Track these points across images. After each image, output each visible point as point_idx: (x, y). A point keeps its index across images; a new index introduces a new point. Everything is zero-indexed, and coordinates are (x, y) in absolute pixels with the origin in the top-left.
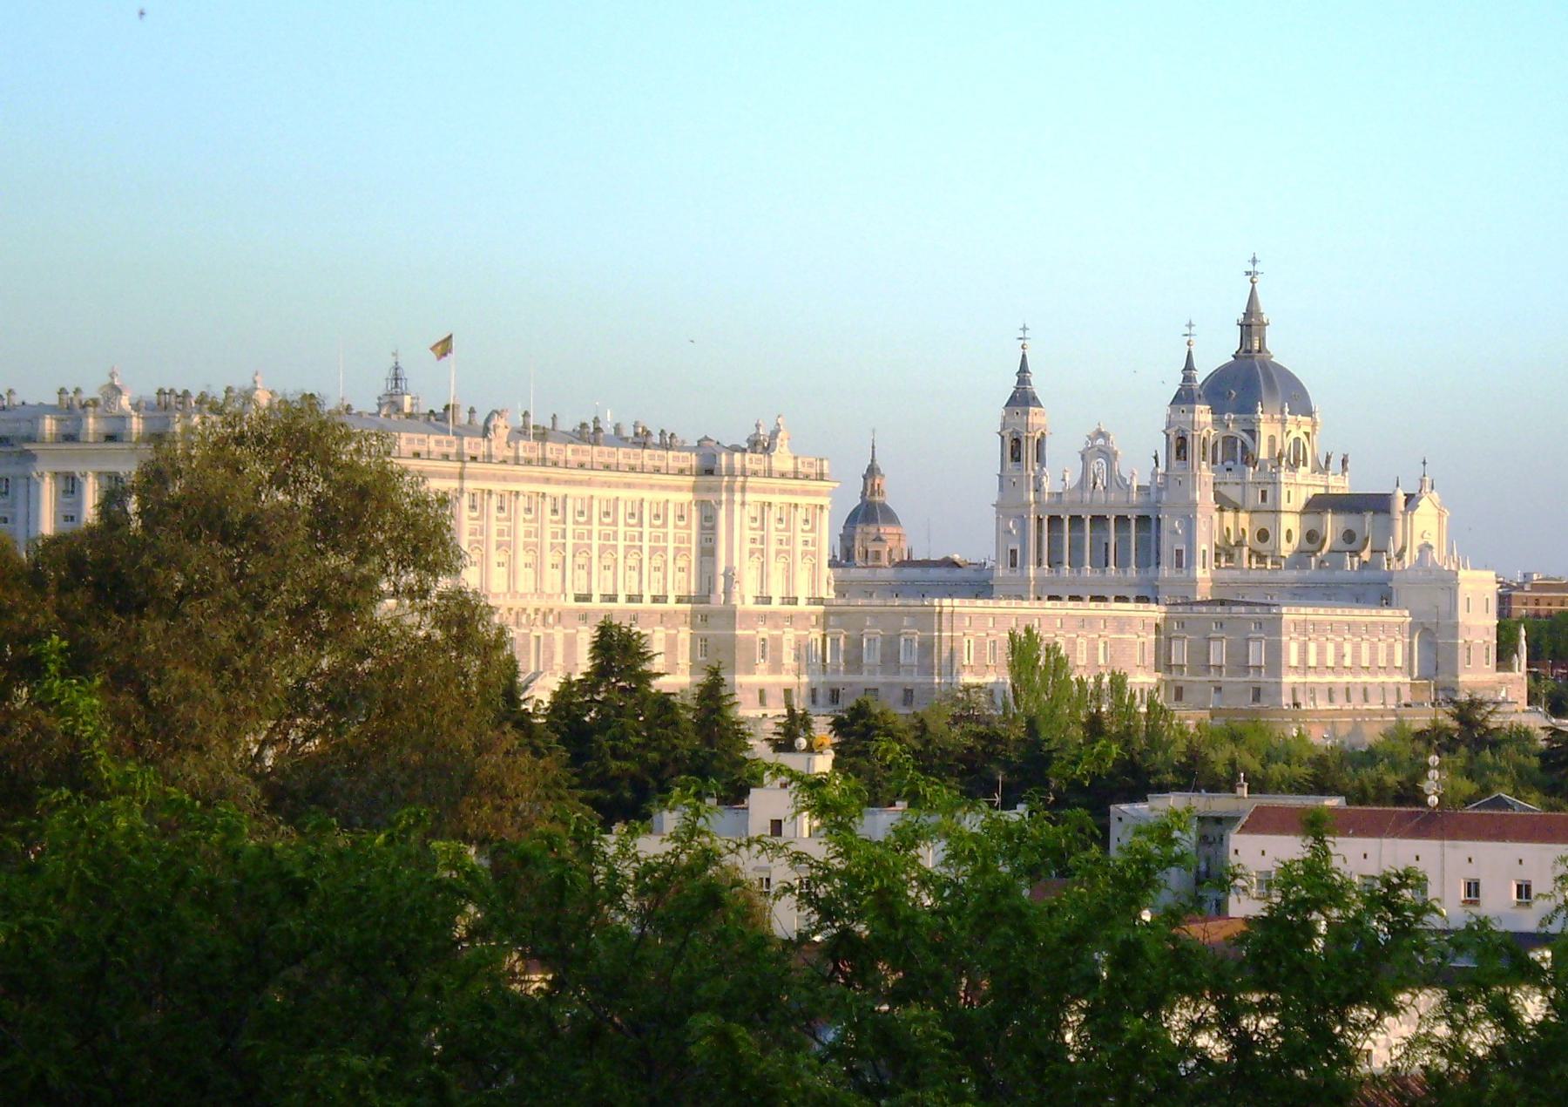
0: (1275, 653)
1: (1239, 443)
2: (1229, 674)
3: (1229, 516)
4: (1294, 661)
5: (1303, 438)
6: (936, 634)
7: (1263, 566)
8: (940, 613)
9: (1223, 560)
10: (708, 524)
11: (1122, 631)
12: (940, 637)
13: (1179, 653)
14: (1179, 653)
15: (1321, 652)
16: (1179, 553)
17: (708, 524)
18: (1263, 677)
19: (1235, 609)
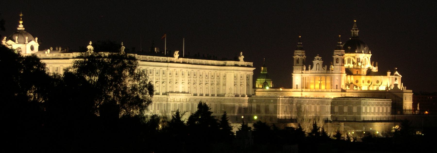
0: (359, 109)
1: (351, 60)
2: (348, 114)
3: (349, 76)
4: (364, 111)
5: (367, 59)
6: (278, 104)
7: (356, 89)
8: (279, 100)
9: (347, 87)
10: (224, 78)
11: (323, 104)
12: (279, 105)
13: (336, 109)
14: (336, 109)
15: (370, 109)
16: (337, 85)
17: (224, 78)
18: (357, 115)
19: (350, 99)
